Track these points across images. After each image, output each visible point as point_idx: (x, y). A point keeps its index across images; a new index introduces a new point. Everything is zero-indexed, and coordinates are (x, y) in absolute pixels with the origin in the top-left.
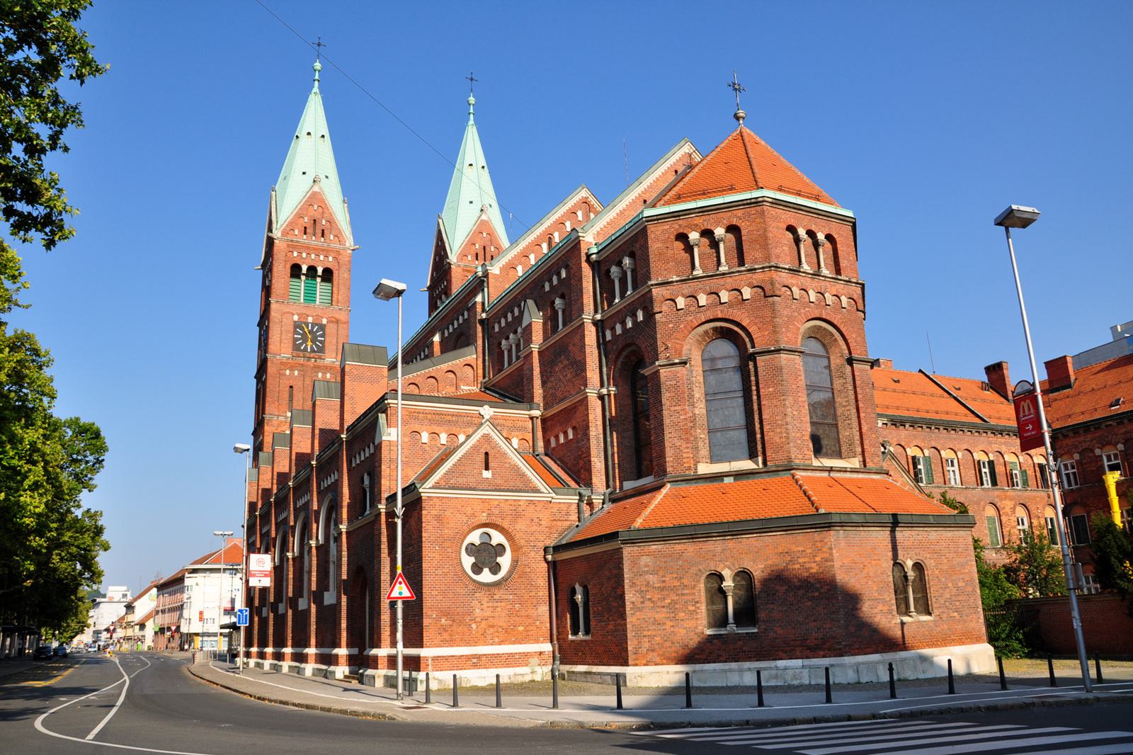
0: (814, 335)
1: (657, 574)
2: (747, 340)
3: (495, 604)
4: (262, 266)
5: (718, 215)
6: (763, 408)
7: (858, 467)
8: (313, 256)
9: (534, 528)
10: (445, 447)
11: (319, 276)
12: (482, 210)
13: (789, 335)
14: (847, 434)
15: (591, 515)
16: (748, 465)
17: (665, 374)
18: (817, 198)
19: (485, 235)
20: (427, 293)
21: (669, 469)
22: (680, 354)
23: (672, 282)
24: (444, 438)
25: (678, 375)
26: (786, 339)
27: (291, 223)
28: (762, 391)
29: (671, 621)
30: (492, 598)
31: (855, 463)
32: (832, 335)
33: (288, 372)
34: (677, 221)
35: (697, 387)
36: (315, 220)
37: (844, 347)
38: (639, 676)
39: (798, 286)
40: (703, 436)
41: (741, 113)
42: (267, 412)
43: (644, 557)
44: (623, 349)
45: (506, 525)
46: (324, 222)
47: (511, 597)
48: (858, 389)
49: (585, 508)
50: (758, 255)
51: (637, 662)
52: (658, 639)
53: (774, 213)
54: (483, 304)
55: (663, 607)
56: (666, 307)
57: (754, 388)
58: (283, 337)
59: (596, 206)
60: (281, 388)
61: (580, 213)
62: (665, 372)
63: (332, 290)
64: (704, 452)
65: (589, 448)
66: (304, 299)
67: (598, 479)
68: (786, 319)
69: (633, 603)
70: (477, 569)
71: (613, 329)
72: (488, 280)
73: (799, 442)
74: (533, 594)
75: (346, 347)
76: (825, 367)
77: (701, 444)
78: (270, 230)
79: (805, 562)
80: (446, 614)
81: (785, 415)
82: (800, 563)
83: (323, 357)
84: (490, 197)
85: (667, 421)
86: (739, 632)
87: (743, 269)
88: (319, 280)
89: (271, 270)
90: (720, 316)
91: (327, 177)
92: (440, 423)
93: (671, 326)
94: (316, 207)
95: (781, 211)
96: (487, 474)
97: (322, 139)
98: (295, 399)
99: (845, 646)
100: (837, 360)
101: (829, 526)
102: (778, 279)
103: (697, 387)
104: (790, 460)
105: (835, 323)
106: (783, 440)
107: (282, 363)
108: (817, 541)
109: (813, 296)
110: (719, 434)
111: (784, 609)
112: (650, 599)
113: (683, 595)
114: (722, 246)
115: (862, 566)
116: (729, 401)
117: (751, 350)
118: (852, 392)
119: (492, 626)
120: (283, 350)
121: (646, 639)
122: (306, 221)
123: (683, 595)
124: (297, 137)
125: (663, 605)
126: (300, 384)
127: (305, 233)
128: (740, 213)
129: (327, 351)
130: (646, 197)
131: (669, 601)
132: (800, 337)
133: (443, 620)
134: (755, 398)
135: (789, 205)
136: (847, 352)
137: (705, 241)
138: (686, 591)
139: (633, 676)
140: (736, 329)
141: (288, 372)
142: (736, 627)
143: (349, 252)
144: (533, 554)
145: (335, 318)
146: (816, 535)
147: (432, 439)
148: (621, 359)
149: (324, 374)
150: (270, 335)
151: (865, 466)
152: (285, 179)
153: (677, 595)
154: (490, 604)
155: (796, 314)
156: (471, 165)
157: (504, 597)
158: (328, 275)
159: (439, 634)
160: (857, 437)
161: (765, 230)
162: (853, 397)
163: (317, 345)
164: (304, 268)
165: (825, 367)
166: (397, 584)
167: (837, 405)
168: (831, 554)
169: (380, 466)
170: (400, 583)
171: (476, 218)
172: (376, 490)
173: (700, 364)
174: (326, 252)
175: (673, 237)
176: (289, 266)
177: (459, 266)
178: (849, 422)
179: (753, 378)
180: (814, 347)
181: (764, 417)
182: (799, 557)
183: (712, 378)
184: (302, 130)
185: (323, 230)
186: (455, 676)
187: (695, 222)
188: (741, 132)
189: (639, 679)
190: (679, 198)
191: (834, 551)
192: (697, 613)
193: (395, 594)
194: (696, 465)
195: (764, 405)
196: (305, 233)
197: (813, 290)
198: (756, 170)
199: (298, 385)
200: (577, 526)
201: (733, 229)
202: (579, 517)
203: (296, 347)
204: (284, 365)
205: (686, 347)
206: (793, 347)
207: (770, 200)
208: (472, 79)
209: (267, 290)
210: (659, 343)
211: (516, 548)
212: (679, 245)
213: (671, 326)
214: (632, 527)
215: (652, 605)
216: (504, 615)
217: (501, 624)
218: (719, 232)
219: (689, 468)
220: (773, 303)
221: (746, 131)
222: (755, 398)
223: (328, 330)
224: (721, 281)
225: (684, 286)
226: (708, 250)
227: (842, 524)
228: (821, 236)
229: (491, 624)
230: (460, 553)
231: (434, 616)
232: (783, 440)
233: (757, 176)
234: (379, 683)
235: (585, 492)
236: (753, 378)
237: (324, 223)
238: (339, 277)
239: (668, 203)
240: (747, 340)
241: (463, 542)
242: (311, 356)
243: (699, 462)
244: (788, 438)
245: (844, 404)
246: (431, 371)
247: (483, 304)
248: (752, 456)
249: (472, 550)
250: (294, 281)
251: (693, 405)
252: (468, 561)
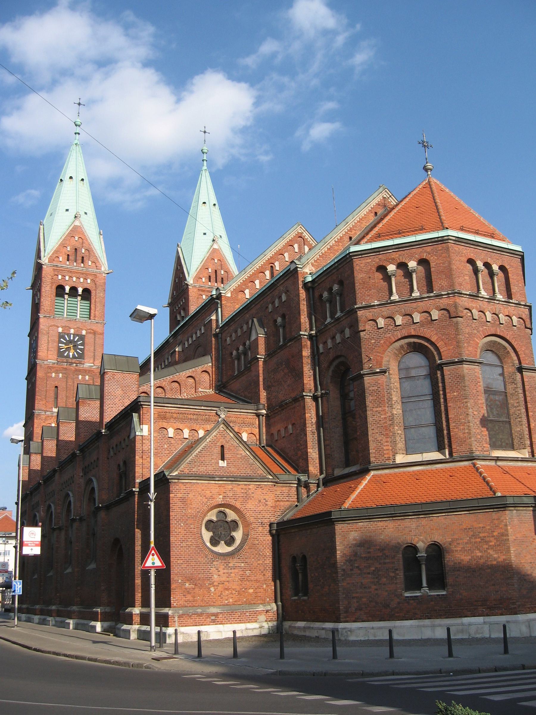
0: (491, 348)
1: (364, 547)
2: (435, 353)
3: (230, 571)
4: (32, 286)
5: (411, 251)
6: (449, 409)
7: (528, 457)
8: (74, 279)
9: (261, 508)
10: (188, 440)
11: (80, 295)
12: (214, 240)
13: (470, 349)
14: (519, 429)
15: (308, 496)
16: (436, 456)
17: (368, 381)
18: (492, 236)
19: (216, 261)
20: (168, 308)
21: (372, 459)
22: (381, 365)
23: (374, 306)
24: (186, 433)
25: (379, 382)
26: (467, 352)
27: (56, 252)
28: (448, 395)
29: (375, 585)
30: (227, 567)
31: (525, 454)
32: (505, 348)
33: (53, 375)
34: (377, 256)
35: (394, 391)
36: (76, 249)
37: (515, 358)
38: (349, 631)
39: (476, 308)
40: (399, 432)
41: (429, 166)
42: (36, 407)
43: (353, 533)
44: (333, 360)
45: (238, 505)
46: (83, 251)
47: (243, 565)
48: (527, 393)
49: (303, 490)
50: (444, 283)
51: (347, 619)
52: (364, 600)
53: (457, 249)
54: (217, 320)
55: (369, 573)
56: (369, 326)
57: (441, 392)
58: (50, 346)
59: (309, 239)
60: (48, 388)
61: (296, 246)
62: (368, 379)
63: (90, 307)
64: (401, 445)
65: (306, 441)
66: (67, 315)
67: (314, 468)
68: (467, 336)
69: (344, 570)
70: (214, 542)
71: (325, 343)
72: (221, 302)
73: (479, 437)
74: (260, 562)
75: (105, 357)
76: (500, 375)
77: (398, 439)
78: (39, 256)
79: (485, 537)
80: (190, 579)
81: (467, 414)
82: (480, 537)
83: (82, 362)
84: (220, 230)
85: (370, 419)
86: (431, 594)
87: (432, 295)
88: (79, 298)
89: (40, 290)
90: (413, 333)
91: (86, 213)
92: (182, 420)
93: (373, 341)
94: (77, 238)
95: (463, 247)
96: (222, 464)
97: (81, 182)
98: (60, 397)
99: (519, 606)
100: (509, 369)
101: (504, 507)
102: (461, 303)
103: (394, 391)
104: (472, 452)
105: (508, 339)
106: (466, 435)
107: (49, 368)
108: (494, 519)
110: (413, 430)
111: (469, 575)
112: (357, 567)
113: (385, 563)
114: (414, 276)
115: (531, 539)
116: (421, 403)
117: (439, 362)
118: (522, 395)
119: (227, 589)
120: (50, 356)
121: (355, 600)
122: (69, 250)
123: (385, 563)
124: (61, 180)
125: (368, 571)
126: (64, 385)
127: (68, 260)
128: (429, 249)
129: (86, 357)
130: (351, 234)
131: (373, 569)
132: (479, 350)
133: (187, 585)
134: (442, 400)
135: (469, 242)
136: (517, 362)
137: (400, 272)
138: (387, 561)
139: (344, 631)
140: (426, 344)
141: (53, 375)
142: (429, 590)
143: (104, 275)
144: (260, 529)
145: (93, 330)
146: (494, 515)
147: (176, 434)
148: (332, 368)
149: (84, 376)
150: (39, 344)
151: (533, 456)
152: (51, 215)
153: (380, 564)
154: (226, 571)
155: (475, 331)
156: (204, 203)
157: (239, 564)
158: (87, 294)
159: (184, 595)
160: (526, 432)
161: (450, 263)
162: (523, 399)
163: (77, 353)
164: (67, 289)
165: (500, 375)
166: (151, 556)
167: (510, 405)
168: (507, 530)
169: (135, 457)
170: (153, 555)
171: (209, 247)
172: (131, 476)
173: (397, 373)
174: (86, 276)
175: (374, 269)
176: (54, 287)
177: (195, 287)
178: (519, 419)
179: (440, 385)
180: (491, 358)
181: (450, 416)
182: (480, 533)
183: (407, 384)
184: (65, 175)
185: (83, 257)
186: (199, 632)
187: (392, 257)
188: (429, 182)
189: (349, 633)
190: (379, 237)
191: (509, 528)
192: (396, 578)
193: (149, 564)
194: (394, 456)
195: (450, 406)
196: (68, 260)
197: (489, 311)
198: (442, 213)
199: (62, 386)
200: (297, 506)
201: (423, 262)
202: (298, 498)
203: (60, 354)
204: (50, 368)
205: (385, 359)
206: (473, 359)
207: (454, 238)
208: (205, 132)
209: (36, 308)
210: (363, 356)
211: (247, 525)
212: (379, 276)
213: (373, 341)
214: (343, 507)
215: (359, 572)
216: (237, 579)
217: (234, 587)
218: (412, 264)
219: (389, 459)
220: (457, 323)
221: (434, 180)
222: (442, 400)
223: (87, 341)
224: (414, 305)
225: (383, 309)
226: (403, 280)
227: (515, 506)
228: (495, 267)
229: (226, 587)
230: (201, 530)
231: (180, 581)
232: (466, 435)
233: (443, 218)
234: (133, 636)
235: (303, 478)
236: (440, 385)
237: (83, 251)
238: (96, 296)
239: (371, 241)
240: (435, 353)
241: (203, 519)
242: (73, 361)
243: (397, 453)
244: (470, 433)
245: (515, 405)
246: (176, 377)
247: (217, 320)
248: (440, 449)
249: (210, 525)
250: (59, 300)
251: (391, 406)
252: (207, 535)
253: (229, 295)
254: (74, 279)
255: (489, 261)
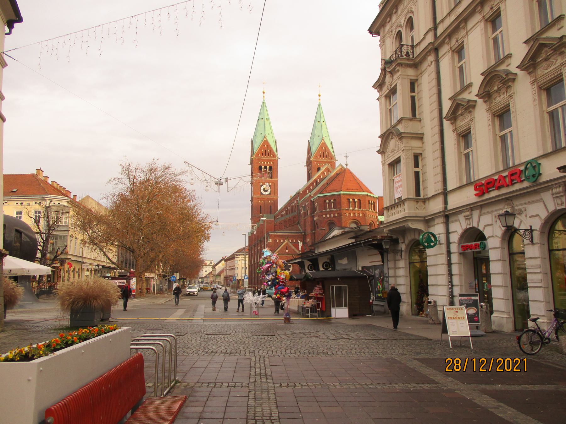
20: (306, 167)
24: (282, 241)
61: (325, 173)
96: (287, 251)
109: (352, 215)
164: (263, 167)
174: (270, 161)
253: (302, 193)
254: (265, 163)
255: (354, 198)
